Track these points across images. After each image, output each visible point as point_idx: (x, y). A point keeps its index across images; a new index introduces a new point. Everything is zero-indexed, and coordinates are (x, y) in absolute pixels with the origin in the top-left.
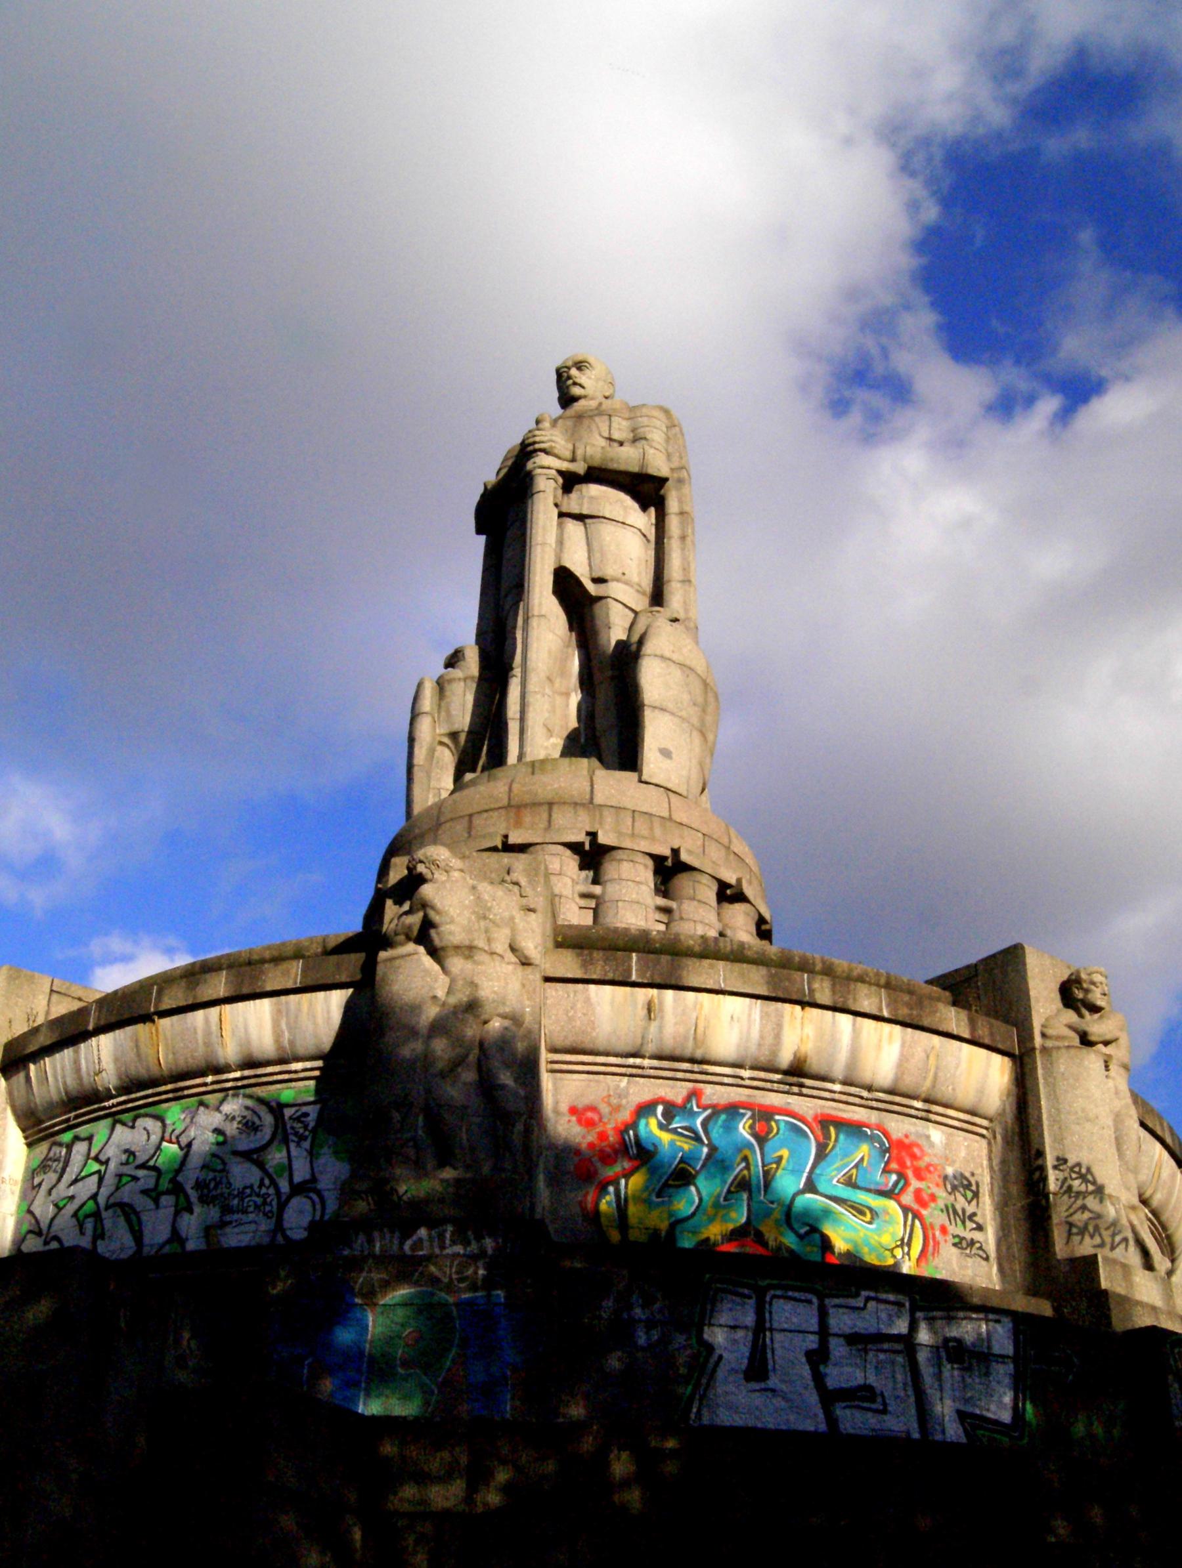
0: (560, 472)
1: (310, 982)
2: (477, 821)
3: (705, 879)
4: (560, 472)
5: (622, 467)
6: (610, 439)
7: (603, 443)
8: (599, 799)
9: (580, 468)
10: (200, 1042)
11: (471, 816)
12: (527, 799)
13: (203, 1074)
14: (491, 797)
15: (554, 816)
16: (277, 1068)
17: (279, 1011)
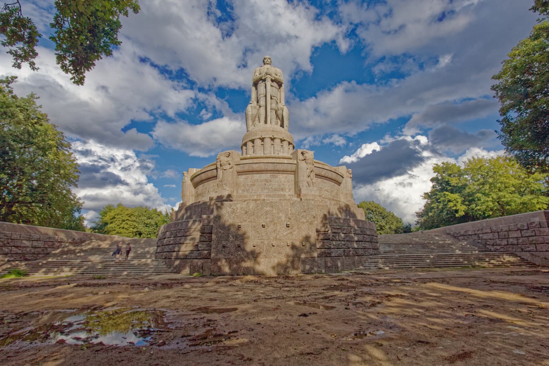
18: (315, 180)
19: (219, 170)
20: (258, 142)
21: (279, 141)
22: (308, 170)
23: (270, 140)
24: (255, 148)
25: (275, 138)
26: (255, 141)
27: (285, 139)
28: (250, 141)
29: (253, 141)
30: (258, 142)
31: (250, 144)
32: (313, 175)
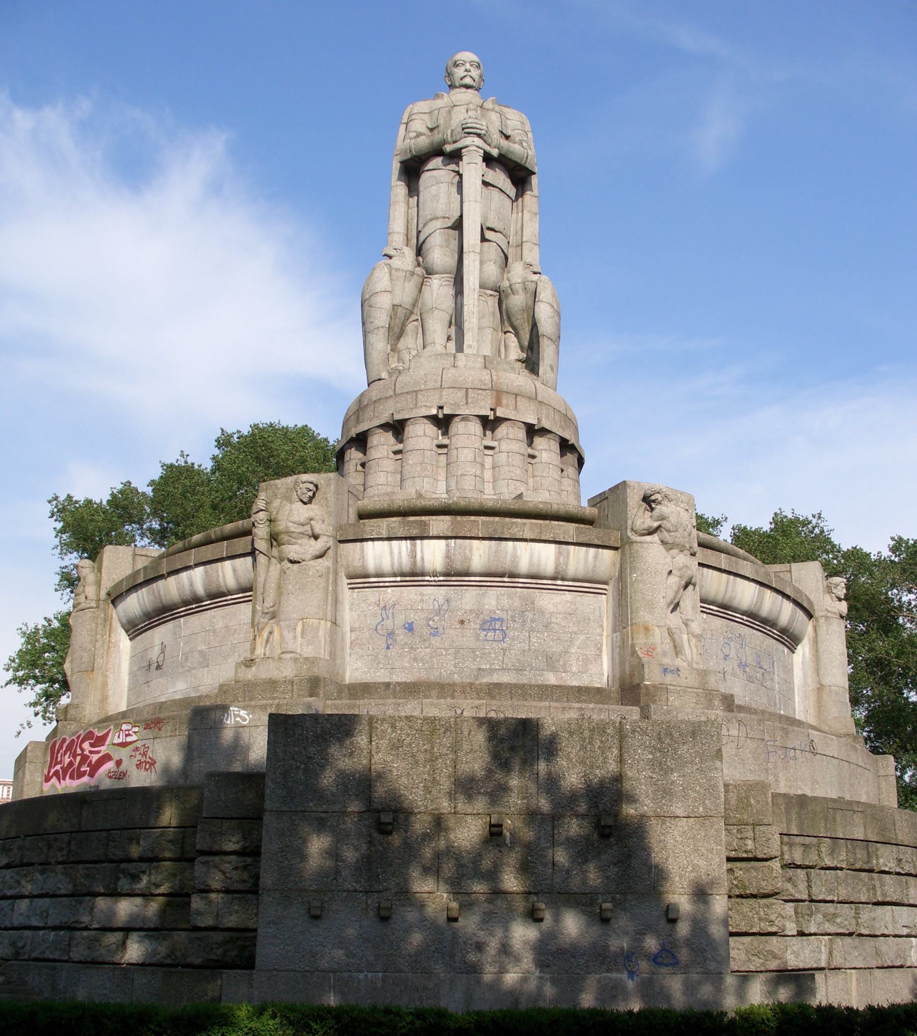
0: (485, 152)
1: (580, 540)
2: (471, 394)
3: (576, 455)
4: (485, 152)
5: (514, 159)
6: (501, 132)
7: (499, 134)
8: (539, 399)
9: (495, 152)
10: (508, 559)
11: (467, 389)
12: (505, 388)
13: (503, 576)
14: (481, 380)
15: (518, 403)
16: (550, 582)
17: (560, 553)
18: (700, 622)
19: (261, 559)
20: (421, 436)
21: (522, 434)
22: (674, 580)
23: (475, 427)
24: (412, 459)
25: (499, 421)
26: (410, 430)
27: (546, 424)
28: (386, 427)
29: (397, 428)
30: (421, 436)
31: (382, 443)
32: (690, 599)
